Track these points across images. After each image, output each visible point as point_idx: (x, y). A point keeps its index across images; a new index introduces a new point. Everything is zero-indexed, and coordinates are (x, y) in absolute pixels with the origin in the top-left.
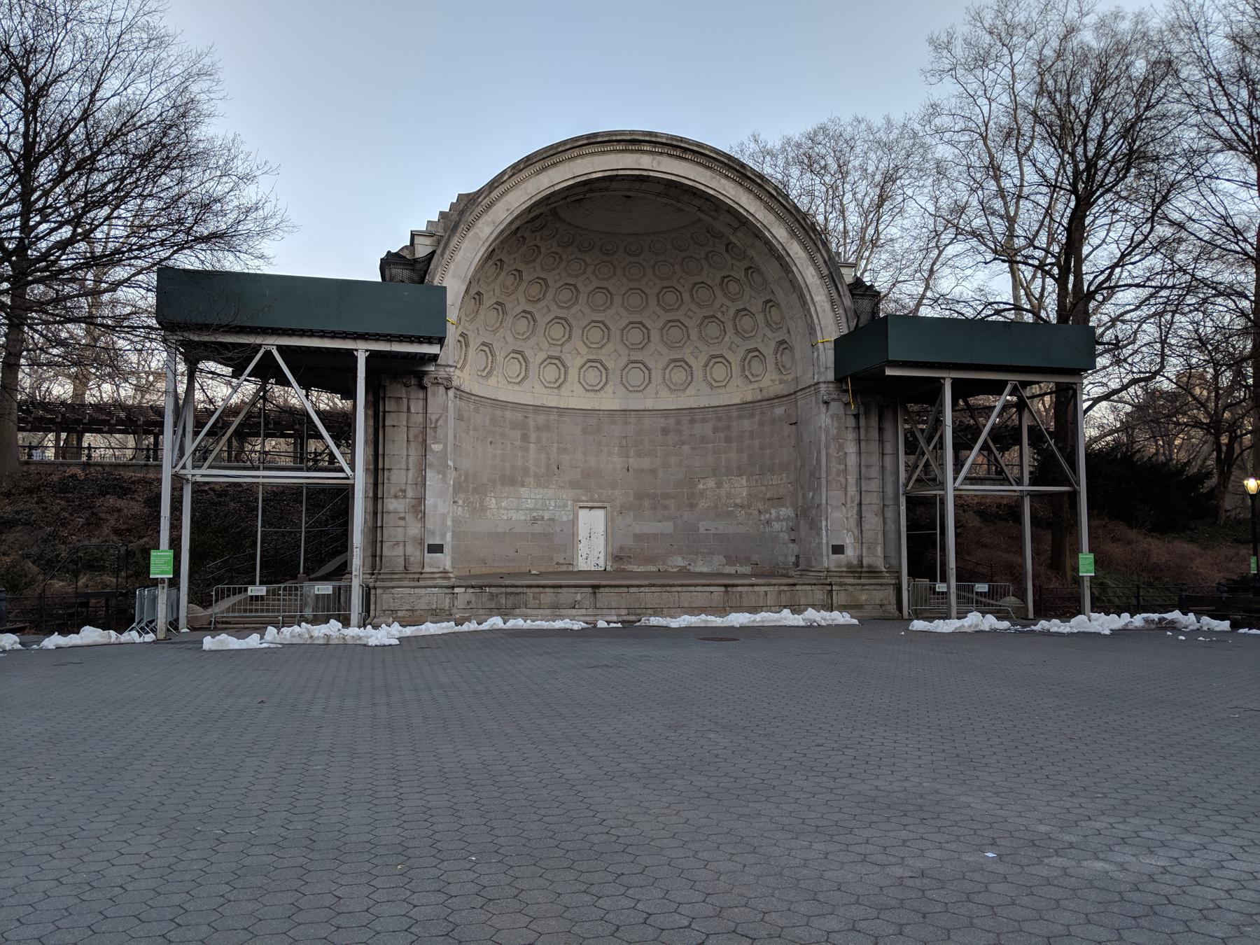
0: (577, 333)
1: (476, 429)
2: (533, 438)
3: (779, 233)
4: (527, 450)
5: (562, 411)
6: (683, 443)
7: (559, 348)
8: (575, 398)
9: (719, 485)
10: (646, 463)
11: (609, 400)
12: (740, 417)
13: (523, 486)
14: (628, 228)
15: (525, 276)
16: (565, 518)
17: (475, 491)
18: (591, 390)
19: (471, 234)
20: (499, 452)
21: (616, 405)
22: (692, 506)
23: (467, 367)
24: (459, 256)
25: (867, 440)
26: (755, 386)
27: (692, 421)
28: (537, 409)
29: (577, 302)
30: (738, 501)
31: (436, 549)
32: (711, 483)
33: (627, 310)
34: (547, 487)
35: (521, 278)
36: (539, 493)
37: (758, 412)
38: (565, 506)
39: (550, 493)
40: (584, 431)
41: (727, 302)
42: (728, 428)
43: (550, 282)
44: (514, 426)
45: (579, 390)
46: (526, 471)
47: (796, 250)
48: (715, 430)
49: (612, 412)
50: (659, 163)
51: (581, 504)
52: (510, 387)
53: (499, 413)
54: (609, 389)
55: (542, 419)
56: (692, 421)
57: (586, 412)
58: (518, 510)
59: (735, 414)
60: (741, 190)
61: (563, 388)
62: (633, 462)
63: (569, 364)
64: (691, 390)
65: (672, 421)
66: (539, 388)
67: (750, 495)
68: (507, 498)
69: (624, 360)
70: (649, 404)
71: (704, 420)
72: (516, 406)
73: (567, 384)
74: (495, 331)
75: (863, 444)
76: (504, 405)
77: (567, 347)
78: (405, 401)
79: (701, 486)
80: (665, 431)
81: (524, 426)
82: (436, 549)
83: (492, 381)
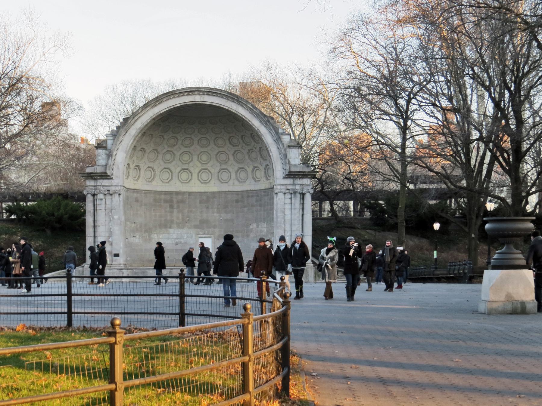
0: (195, 158)
1: (145, 205)
2: (175, 206)
3: (256, 123)
4: (172, 212)
5: (190, 194)
6: (244, 207)
7: (187, 165)
8: (196, 187)
9: (258, 226)
10: (229, 216)
11: (213, 187)
12: (265, 195)
13: (170, 228)
14: (194, 123)
15: (165, 137)
16: (192, 242)
17: (146, 231)
18: (204, 182)
19: (127, 134)
20: (158, 214)
21: (215, 189)
22: (248, 236)
23: (140, 179)
24: (123, 143)
25: (295, 209)
26: (268, 181)
27: (248, 197)
28: (177, 193)
29: (193, 144)
30: (264, 234)
31: (117, 255)
32: (254, 226)
33: (217, 146)
34: (183, 228)
35: (164, 138)
36: (180, 231)
38: (192, 237)
39: (185, 231)
40: (201, 202)
41: (256, 144)
42: (261, 200)
43: (179, 138)
44: (166, 201)
45: (198, 182)
46: (172, 222)
47: (263, 130)
48: (257, 201)
49: (214, 193)
50: (203, 98)
51: (200, 236)
52: (163, 184)
53: (158, 196)
54: (212, 182)
55: (180, 197)
56: (248, 197)
57: (201, 194)
58: (168, 239)
59: (263, 194)
61: (191, 182)
62: (224, 216)
63: (193, 172)
64: (248, 182)
65: (240, 196)
66: (178, 183)
67: (267, 231)
68: (162, 234)
69: (218, 169)
70: (231, 189)
71: (252, 196)
72: (166, 193)
73: (192, 181)
74: (154, 161)
75: (293, 210)
76: (160, 193)
77: (191, 164)
78: (104, 200)
79: (251, 227)
80: (237, 201)
81: (171, 201)
82: (117, 255)
83: (154, 183)
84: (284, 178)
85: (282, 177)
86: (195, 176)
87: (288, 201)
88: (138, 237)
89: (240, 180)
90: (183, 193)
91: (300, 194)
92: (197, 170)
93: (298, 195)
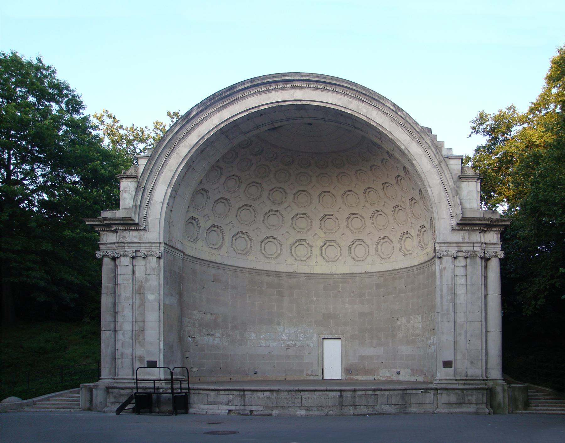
3: (401, 136)
5: (309, 276)
37: (426, 269)
60: (371, 108)
65: (382, 279)
66: (290, 260)
72: (271, 273)
76: (261, 272)
80: (378, 286)
84: (453, 230)
85: (450, 229)
86: (316, 251)
87: (460, 271)
88: (218, 335)
89: (383, 256)
90: (297, 275)
91: (482, 258)
92: (320, 243)
93: (478, 260)
